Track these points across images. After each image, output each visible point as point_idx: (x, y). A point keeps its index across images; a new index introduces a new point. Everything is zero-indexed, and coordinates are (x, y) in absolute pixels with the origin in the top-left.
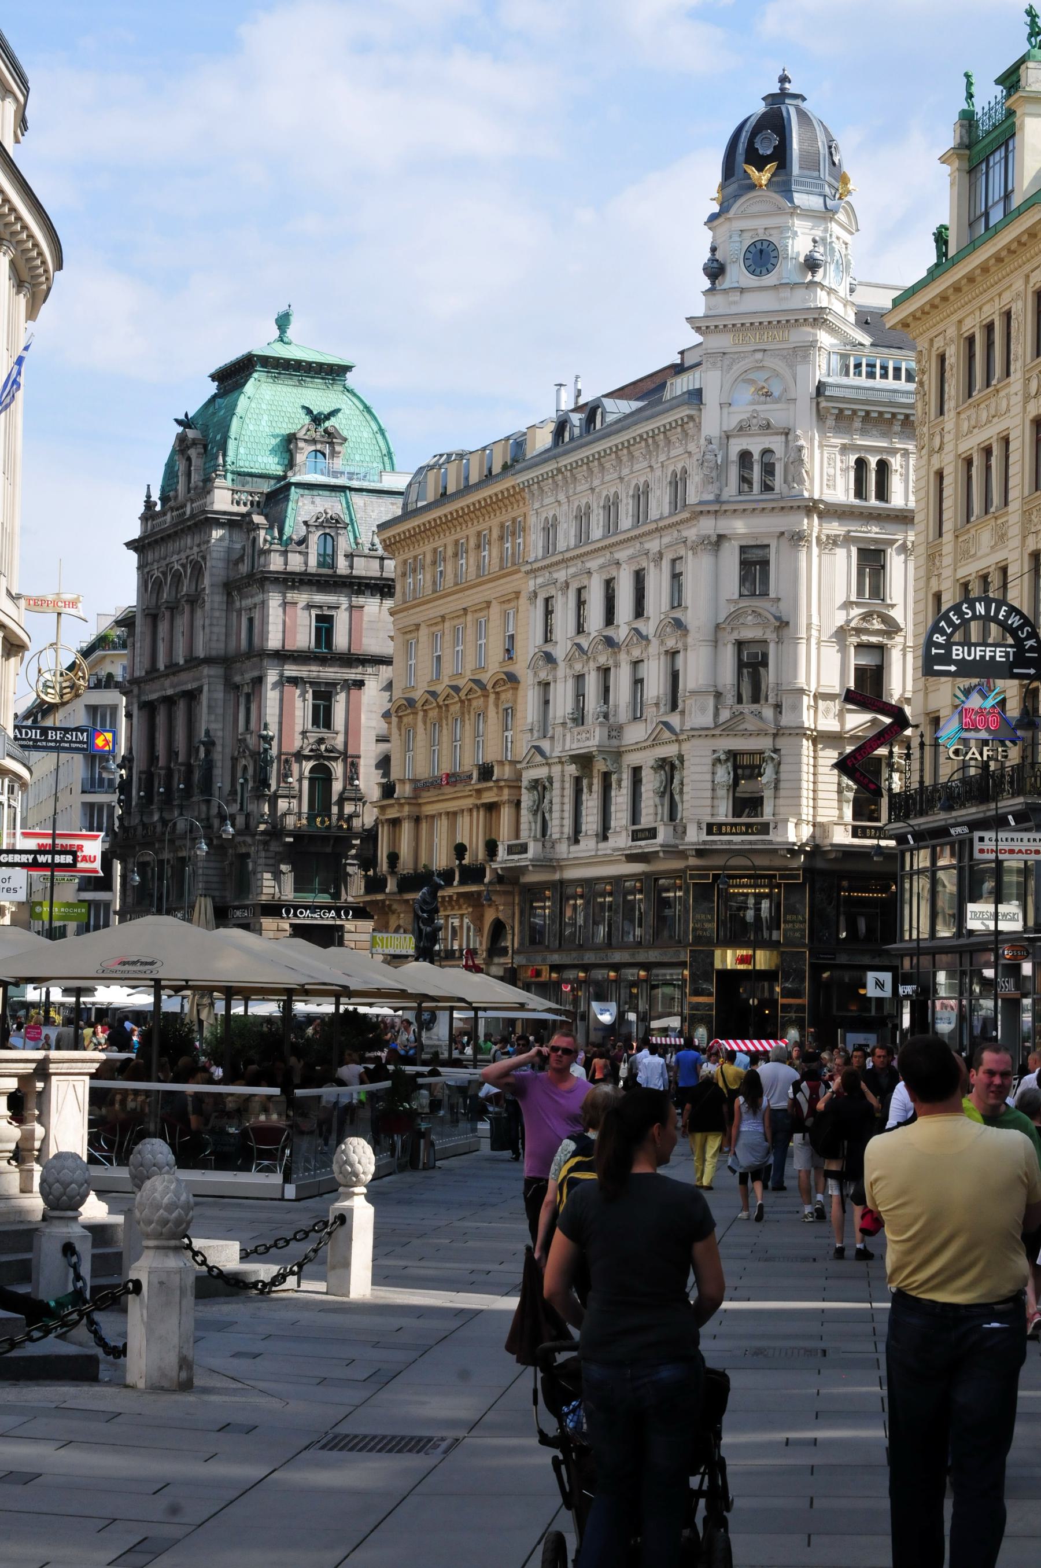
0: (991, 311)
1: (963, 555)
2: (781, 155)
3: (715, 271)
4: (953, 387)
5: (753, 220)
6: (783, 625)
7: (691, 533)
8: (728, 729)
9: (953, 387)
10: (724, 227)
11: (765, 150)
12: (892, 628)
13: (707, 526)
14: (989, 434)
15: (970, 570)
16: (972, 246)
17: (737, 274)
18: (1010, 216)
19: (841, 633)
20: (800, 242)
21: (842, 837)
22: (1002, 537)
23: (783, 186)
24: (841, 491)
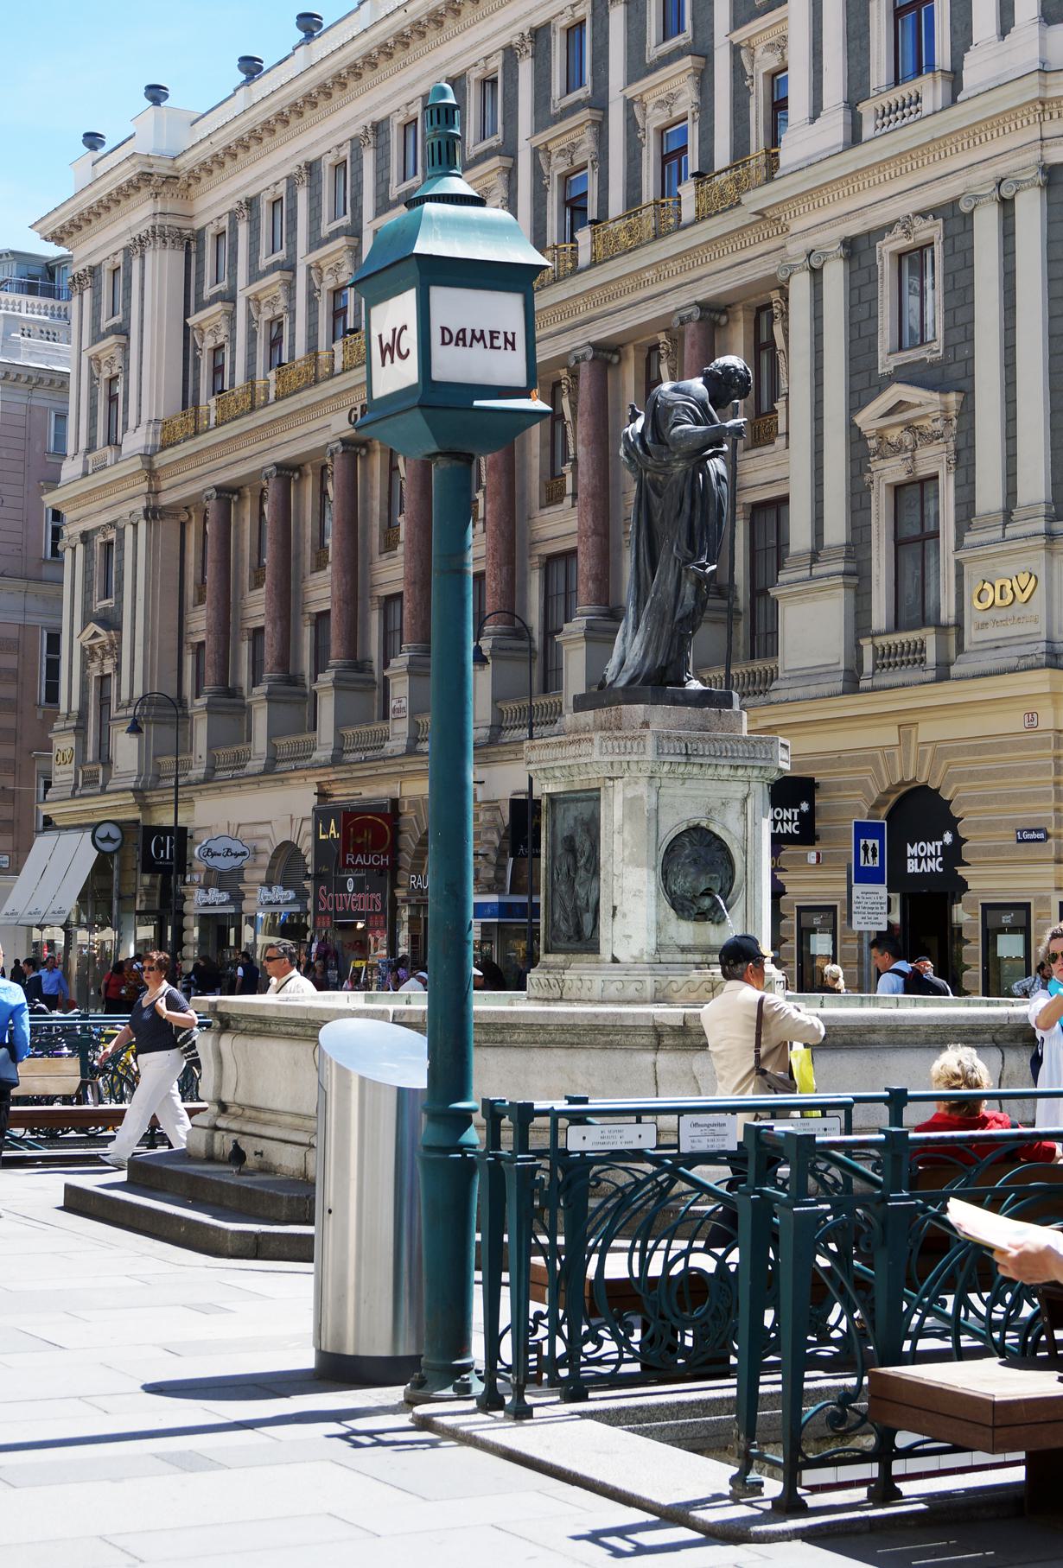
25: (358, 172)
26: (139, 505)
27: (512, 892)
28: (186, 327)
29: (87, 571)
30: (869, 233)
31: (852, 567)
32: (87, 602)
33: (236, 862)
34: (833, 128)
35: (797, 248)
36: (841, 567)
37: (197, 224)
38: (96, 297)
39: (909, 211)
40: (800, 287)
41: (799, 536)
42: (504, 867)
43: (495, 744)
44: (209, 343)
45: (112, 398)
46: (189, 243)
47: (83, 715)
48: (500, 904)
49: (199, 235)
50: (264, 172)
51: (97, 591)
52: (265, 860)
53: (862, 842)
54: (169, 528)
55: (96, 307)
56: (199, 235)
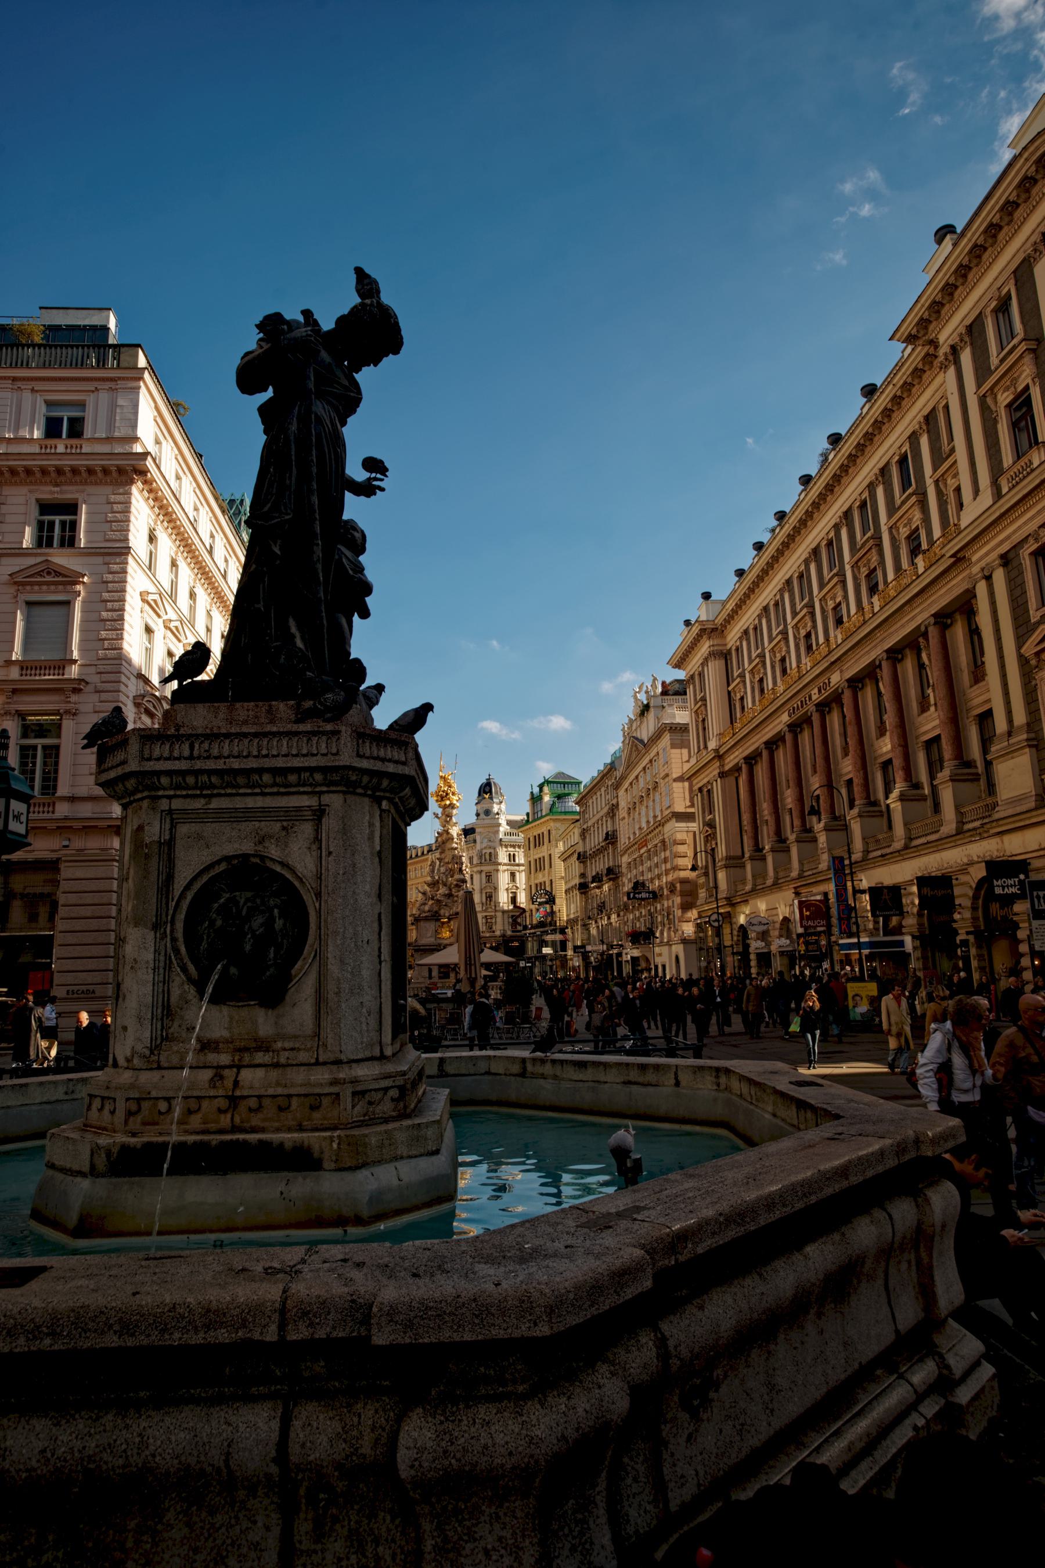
0: (540, 832)
1: (535, 878)
2: (490, 792)
3: (478, 815)
4: (532, 845)
5: (484, 805)
6: (496, 889)
7: (475, 869)
8: (485, 911)
9: (532, 845)
10: (479, 806)
11: (487, 789)
12: (517, 888)
13: (479, 868)
14: (541, 855)
15: (538, 881)
16: (534, 820)
17: (482, 816)
18: (542, 817)
19: (507, 890)
20: (496, 808)
21: (509, 933)
22: (544, 876)
23: (491, 798)
24: (506, 860)
25: (784, 605)
26: (716, 772)
27: (885, 935)
28: (729, 693)
29: (703, 804)
30: (1014, 547)
31: (1033, 735)
32: (704, 817)
33: (765, 928)
34: (986, 498)
35: (975, 569)
36: (1025, 736)
37: (728, 647)
38: (694, 687)
39: (1035, 527)
40: (981, 589)
41: (1001, 724)
42: (878, 923)
43: (866, 862)
44: (738, 696)
45: (704, 729)
46: (725, 656)
47: (707, 867)
48: (870, 942)
49: (729, 651)
50: (748, 618)
51: (707, 813)
52: (778, 926)
53: (1035, 894)
54: (731, 780)
55: (695, 691)
56: (729, 651)
